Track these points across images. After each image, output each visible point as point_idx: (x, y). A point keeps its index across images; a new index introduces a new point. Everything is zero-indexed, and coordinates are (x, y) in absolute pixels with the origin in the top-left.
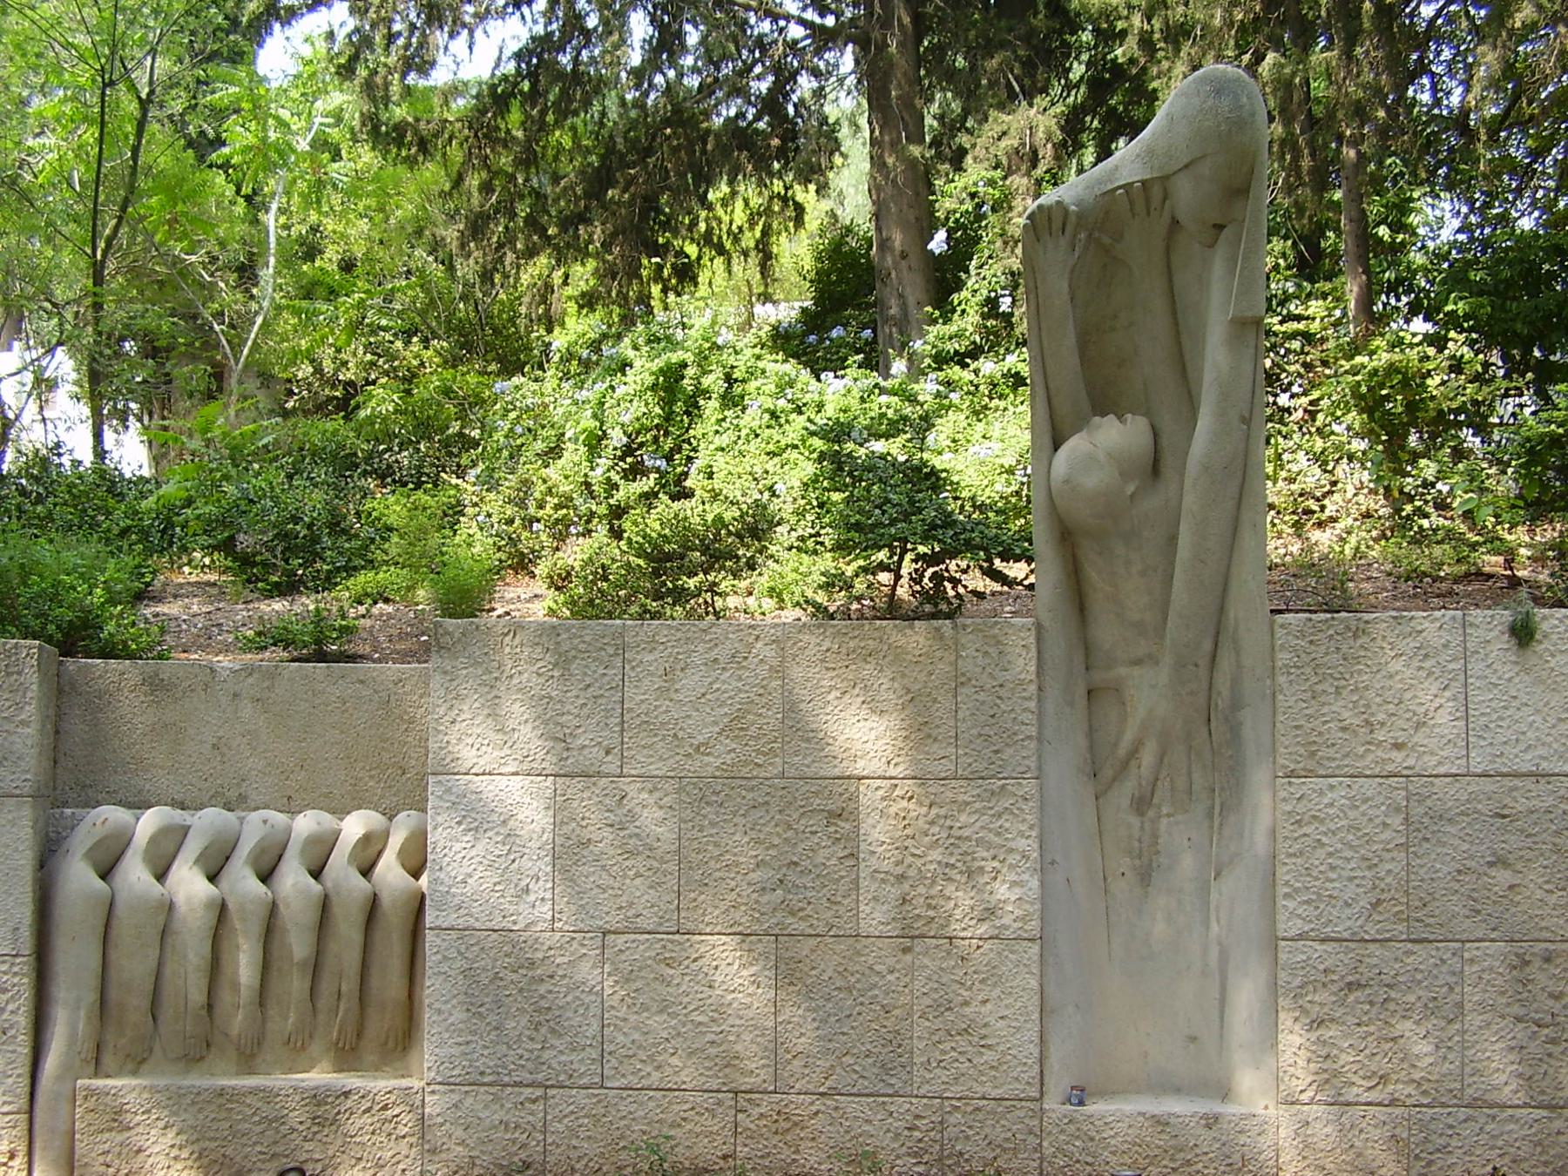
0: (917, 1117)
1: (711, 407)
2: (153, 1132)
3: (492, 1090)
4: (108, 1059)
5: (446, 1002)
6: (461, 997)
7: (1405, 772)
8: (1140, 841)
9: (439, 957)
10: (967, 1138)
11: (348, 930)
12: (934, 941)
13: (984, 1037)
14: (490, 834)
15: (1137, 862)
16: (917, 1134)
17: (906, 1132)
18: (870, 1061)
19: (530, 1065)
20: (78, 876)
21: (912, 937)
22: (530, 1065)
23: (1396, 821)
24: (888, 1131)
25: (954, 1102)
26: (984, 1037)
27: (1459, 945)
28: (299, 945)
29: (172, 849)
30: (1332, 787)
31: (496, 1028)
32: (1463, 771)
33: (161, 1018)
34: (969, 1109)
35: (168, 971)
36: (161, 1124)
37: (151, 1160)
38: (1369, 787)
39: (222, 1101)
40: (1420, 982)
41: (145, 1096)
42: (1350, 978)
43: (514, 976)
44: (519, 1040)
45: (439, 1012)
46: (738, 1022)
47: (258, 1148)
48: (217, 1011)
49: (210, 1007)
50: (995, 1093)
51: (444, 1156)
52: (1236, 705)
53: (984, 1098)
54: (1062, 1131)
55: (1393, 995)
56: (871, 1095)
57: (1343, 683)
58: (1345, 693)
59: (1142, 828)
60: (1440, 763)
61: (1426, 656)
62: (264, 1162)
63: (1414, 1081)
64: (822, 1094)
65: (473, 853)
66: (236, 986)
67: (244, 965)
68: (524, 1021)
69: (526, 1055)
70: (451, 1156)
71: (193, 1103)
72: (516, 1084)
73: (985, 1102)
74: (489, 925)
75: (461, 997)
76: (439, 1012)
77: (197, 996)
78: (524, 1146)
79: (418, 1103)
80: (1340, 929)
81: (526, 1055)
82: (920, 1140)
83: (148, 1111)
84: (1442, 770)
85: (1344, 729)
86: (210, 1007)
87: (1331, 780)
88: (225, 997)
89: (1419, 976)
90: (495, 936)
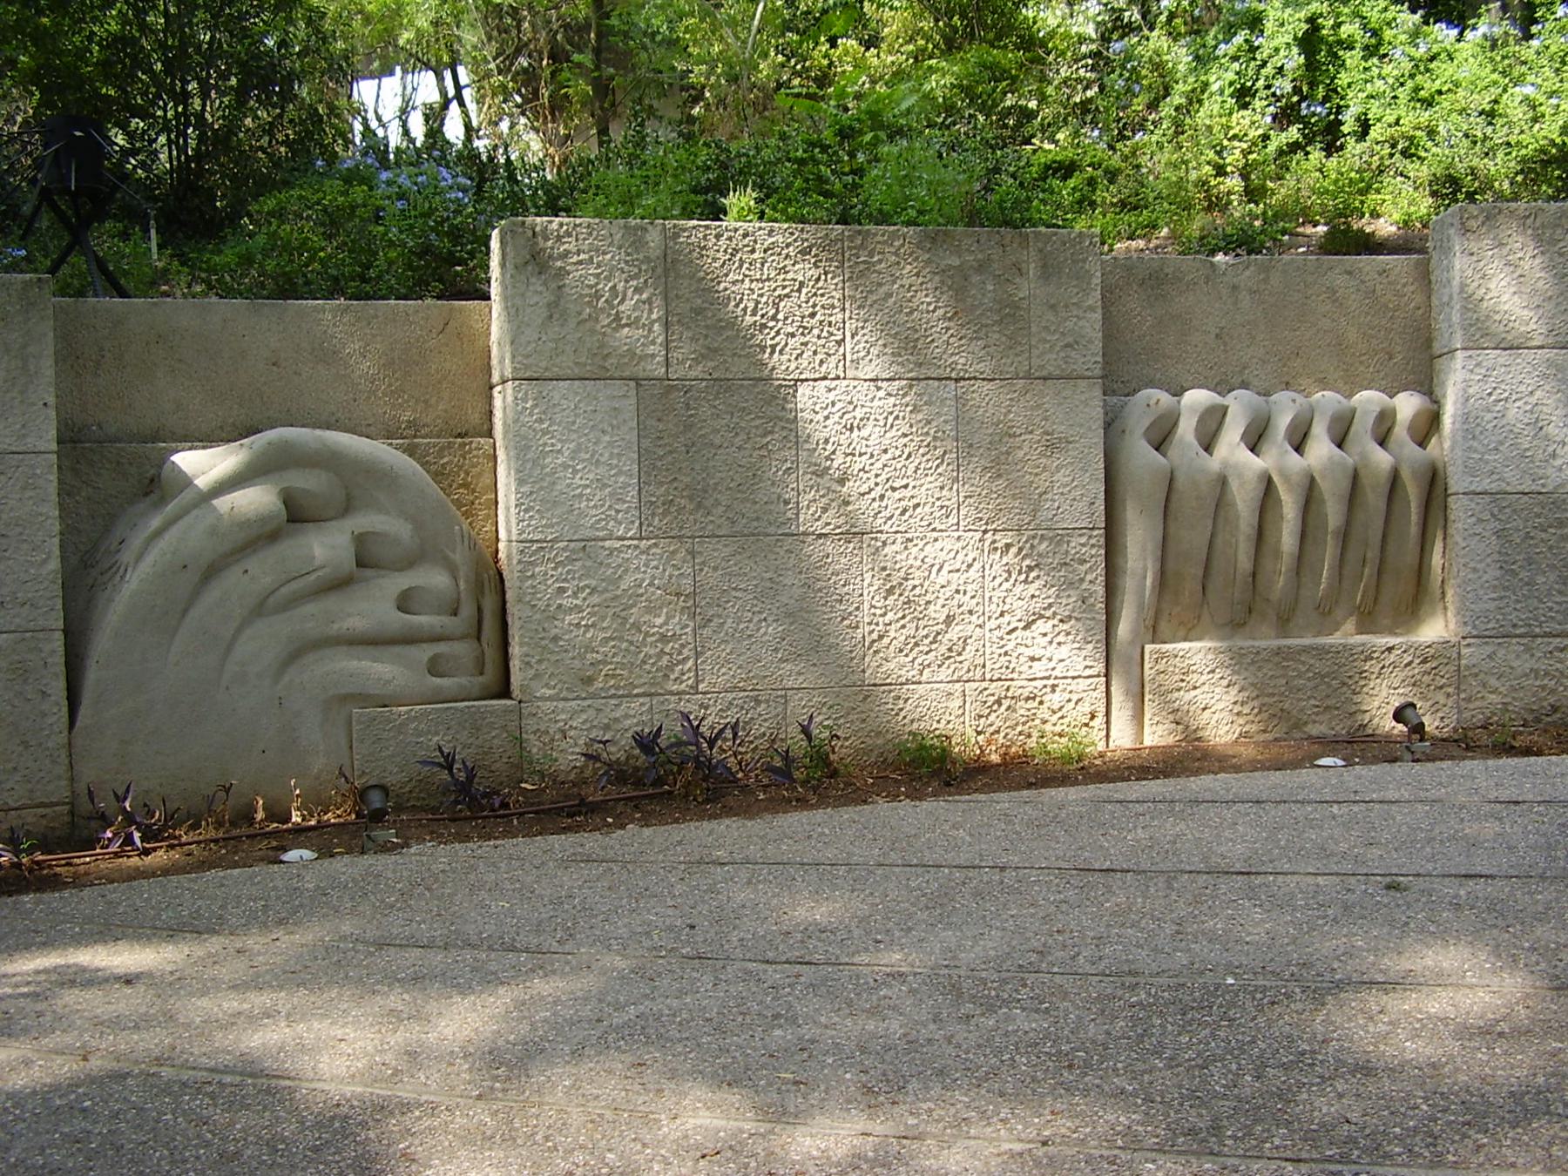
1: (1352, 58)
2: (1217, 690)
3: (1525, 641)
4: (1163, 626)
5: (1481, 561)
6: (1496, 557)
9: (1473, 519)
11: (1374, 500)
14: (1518, 404)
19: (1559, 617)
20: (1140, 455)
22: (1559, 617)
28: (1334, 514)
29: (1214, 427)
31: (1527, 584)
33: (1210, 587)
35: (1219, 541)
36: (1225, 682)
37: (1216, 717)
39: (1277, 659)
41: (1210, 657)
43: (1543, 535)
44: (1549, 595)
45: (1475, 570)
47: (1313, 702)
48: (1259, 577)
49: (1254, 575)
51: (1478, 704)
62: (1317, 714)
65: (1504, 422)
66: (1277, 554)
67: (1287, 537)
68: (1552, 577)
69: (1556, 607)
70: (1485, 704)
71: (1253, 662)
72: (1546, 635)
74: (1520, 488)
75: (1496, 557)
76: (1475, 570)
77: (1244, 562)
78: (1552, 691)
79: (1455, 655)
81: (1556, 607)
83: (1213, 671)
86: (1254, 575)
88: (1267, 563)
90: (1526, 498)
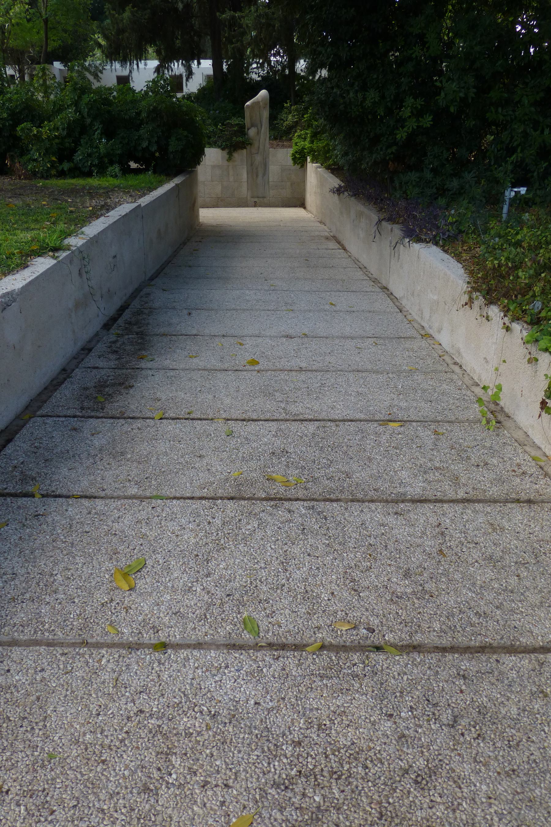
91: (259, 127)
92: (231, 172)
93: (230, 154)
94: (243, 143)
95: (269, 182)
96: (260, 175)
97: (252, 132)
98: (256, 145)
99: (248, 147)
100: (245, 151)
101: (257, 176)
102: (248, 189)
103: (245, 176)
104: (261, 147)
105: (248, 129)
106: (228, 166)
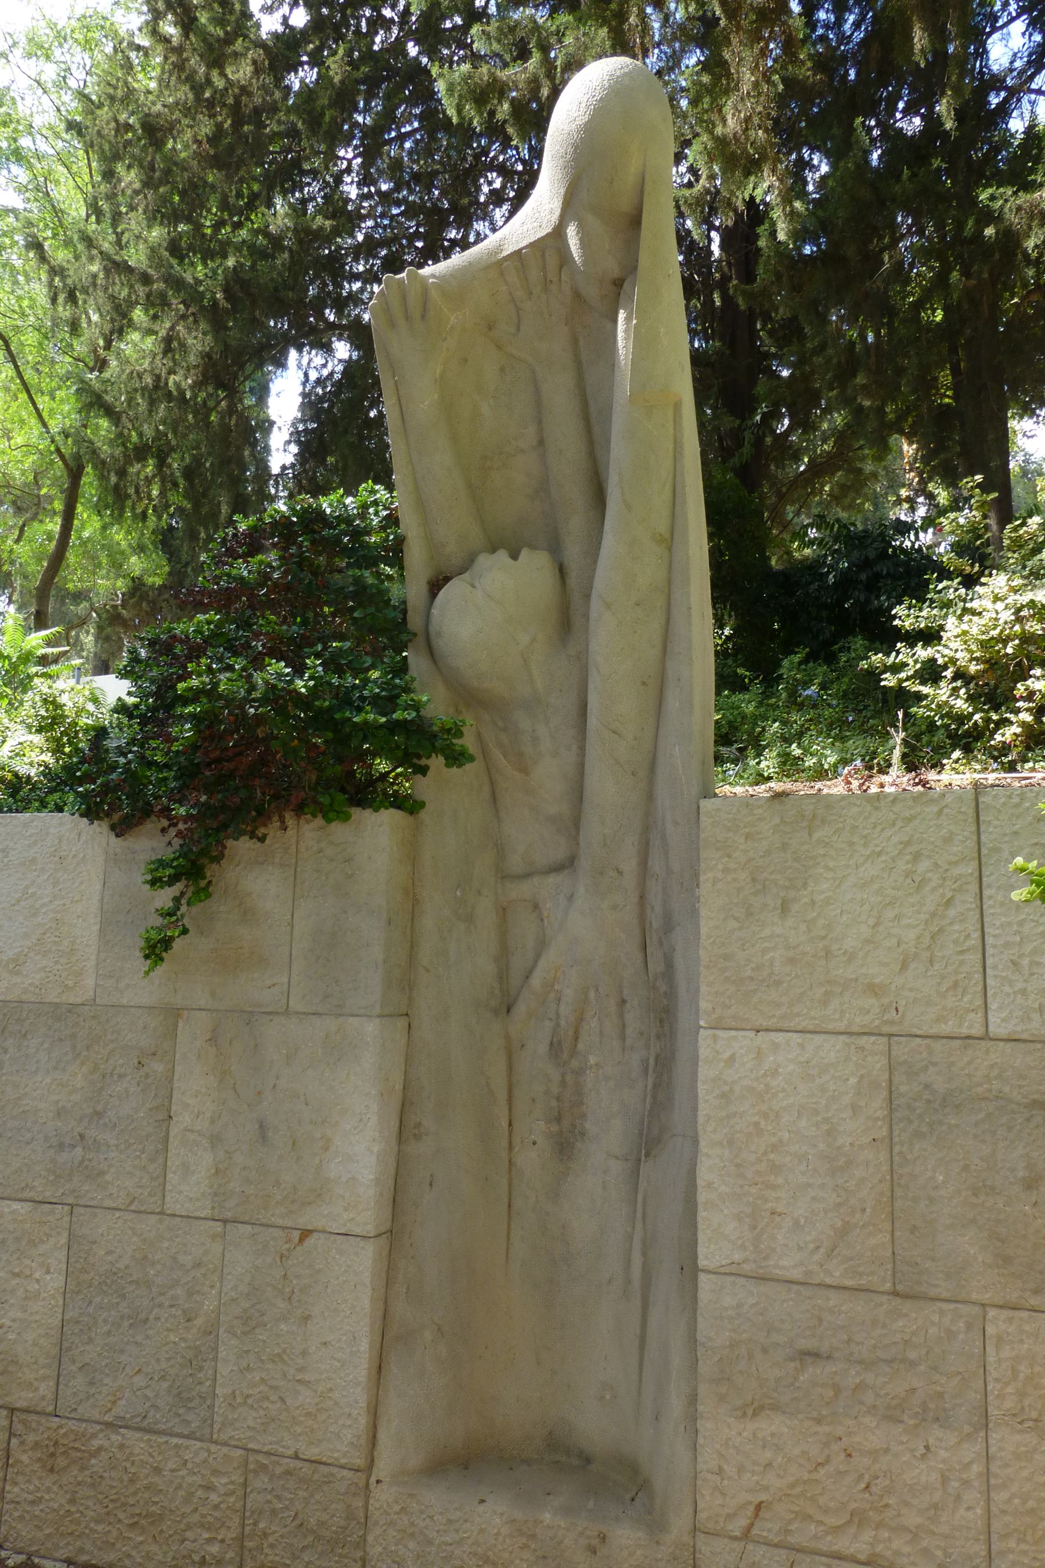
0: (216, 1472)
7: (886, 1029)
8: (558, 1099)
10: (274, 1512)
12: (249, 1227)
13: (302, 1369)
15: (555, 1128)
16: (214, 1498)
17: (200, 1493)
18: (165, 1385)
21: (225, 1222)
23: (877, 1105)
24: (179, 1487)
25: (261, 1458)
26: (302, 1369)
27: (977, 1309)
30: (776, 1046)
32: (977, 1030)
34: (278, 1470)
38: (831, 1048)
40: (913, 1364)
42: (803, 1344)
46: (19, 1315)
50: (312, 1453)
52: (668, 925)
53: (296, 1457)
54: (392, 1523)
55: (869, 1378)
56: (162, 1433)
57: (792, 894)
58: (795, 907)
59: (563, 1083)
60: (940, 1019)
61: (917, 857)
63: (906, 1529)
64: (108, 1425)
73: (300, 1464)
80: (788, 1265)
82: (216, 1507)
84: (946, 1029)
85: (791, 961)
87: (773, 1035)
89: (912, 1355)
91: (573, 552)
92: (194, 1093)
93: (191, 871)
94: (325, 715)
95: (689, 1270)
96: (608, 1131)
97: (480, 619)
98: (549, 775)
99: (439, 785)
100: (376, 831)
101: (566, 1144)
102: (389, 1340)
103: (357, 1156)
104: (608, 789)
105: (435, 586)
106: (173, 1014)
